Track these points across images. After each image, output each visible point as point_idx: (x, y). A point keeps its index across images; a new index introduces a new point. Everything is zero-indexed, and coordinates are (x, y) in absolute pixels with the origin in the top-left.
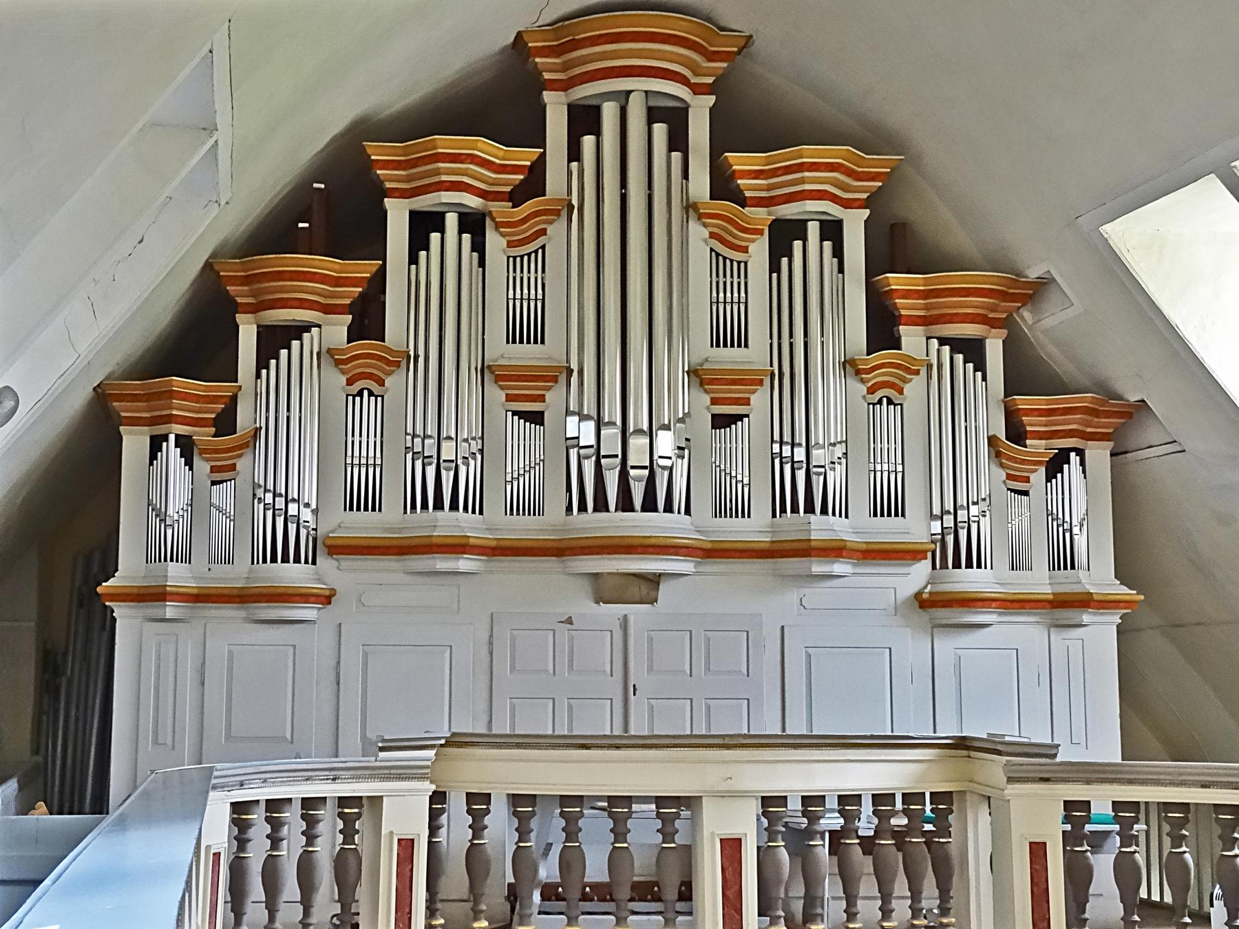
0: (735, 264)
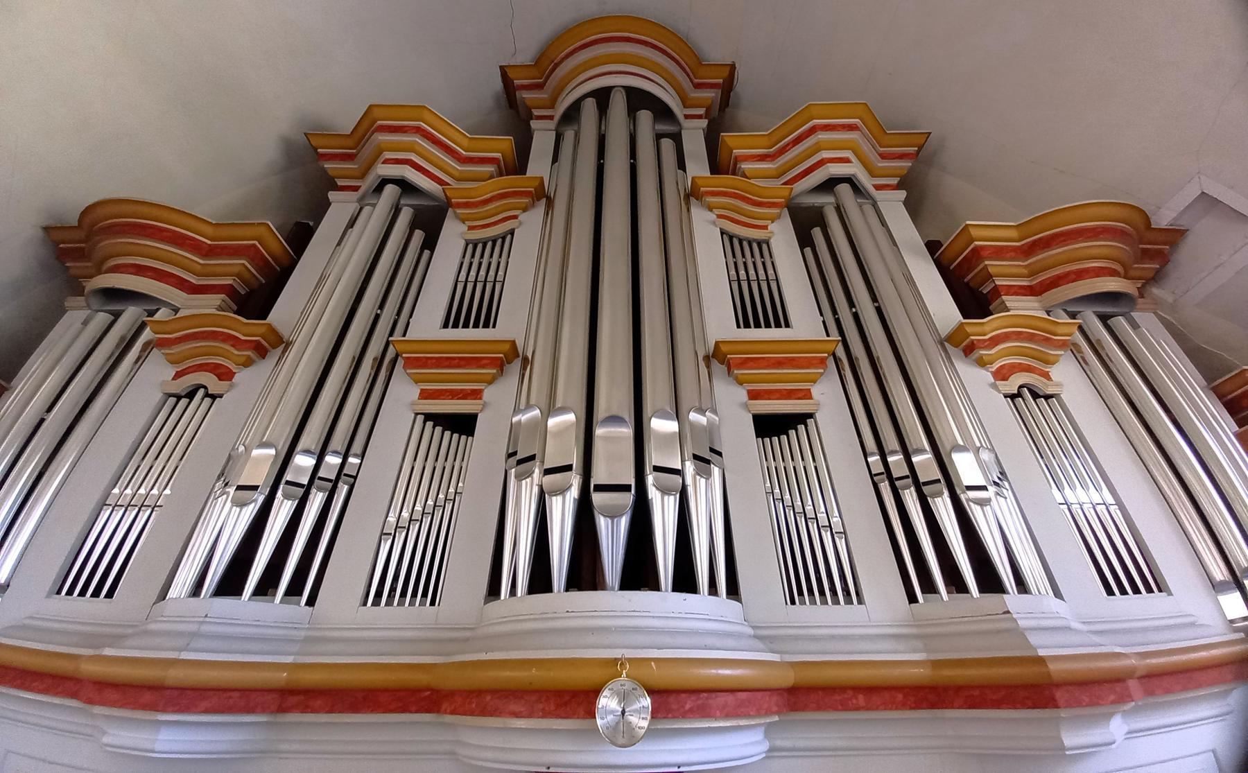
0: (755, 246)
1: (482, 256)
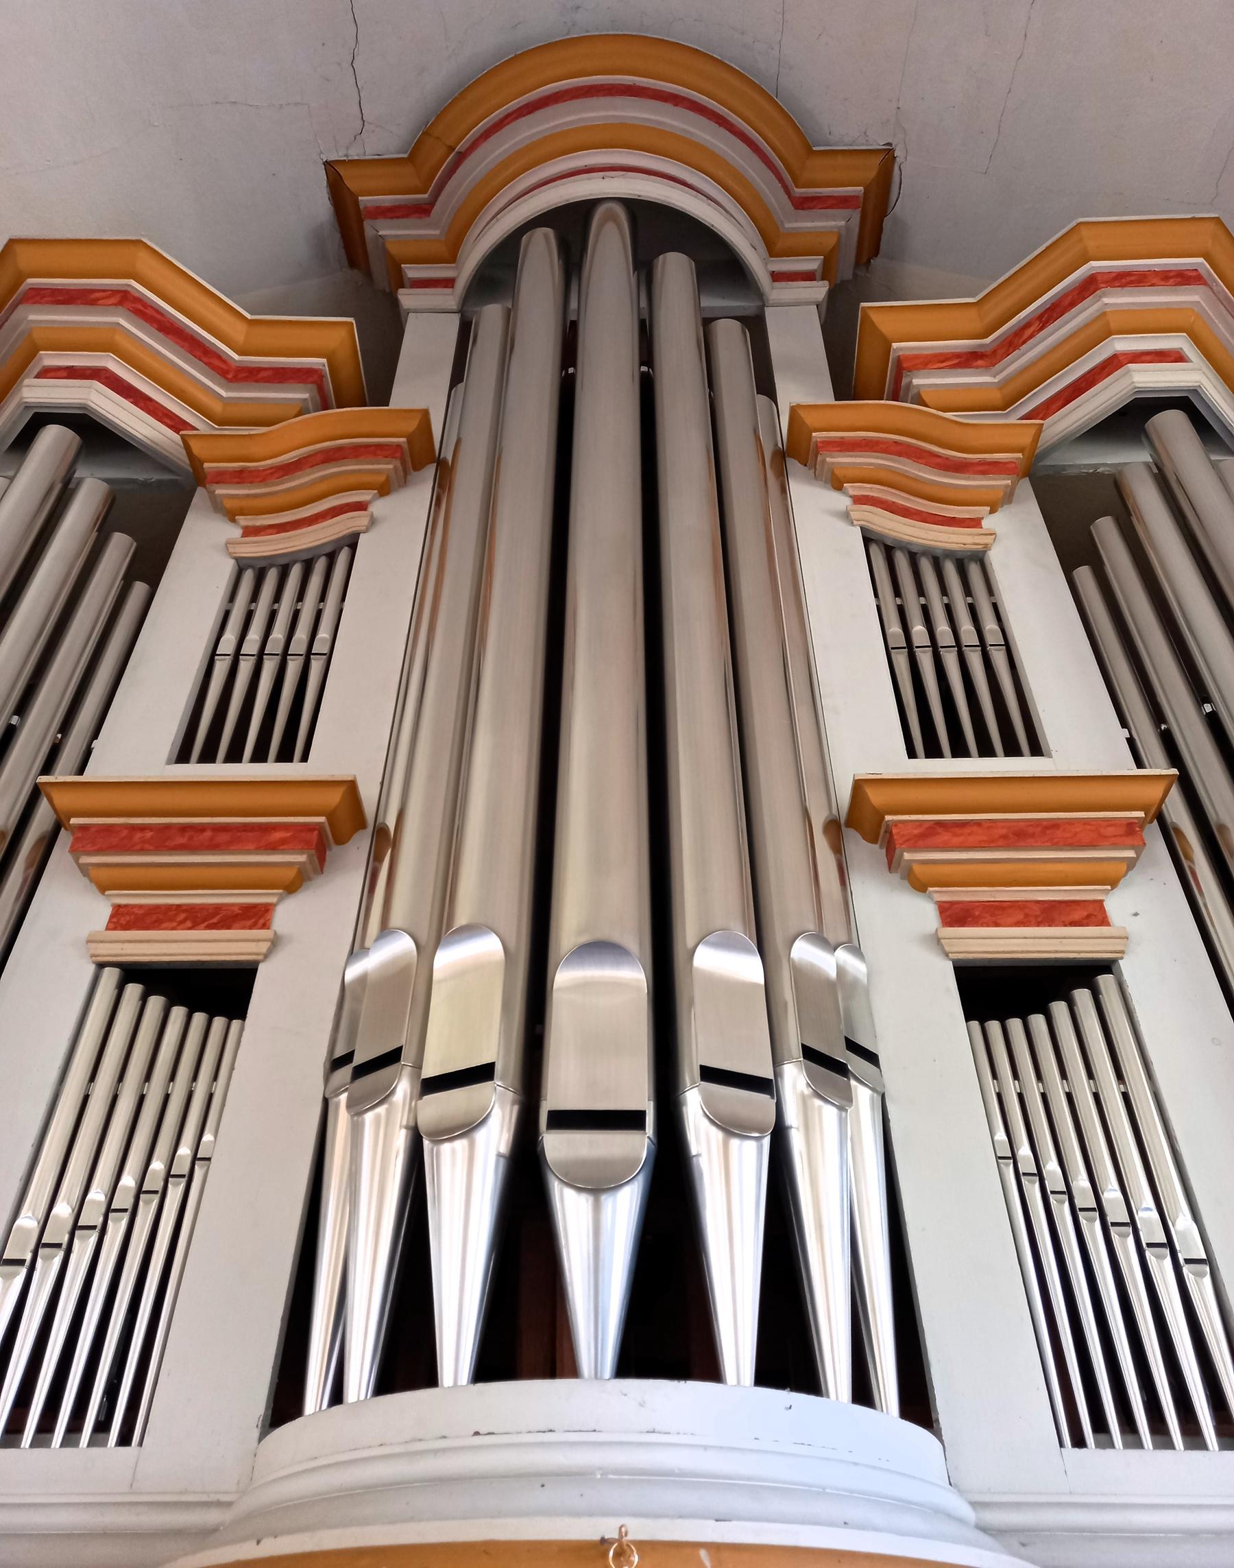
0: (950, 570)
1: (277, 598)
